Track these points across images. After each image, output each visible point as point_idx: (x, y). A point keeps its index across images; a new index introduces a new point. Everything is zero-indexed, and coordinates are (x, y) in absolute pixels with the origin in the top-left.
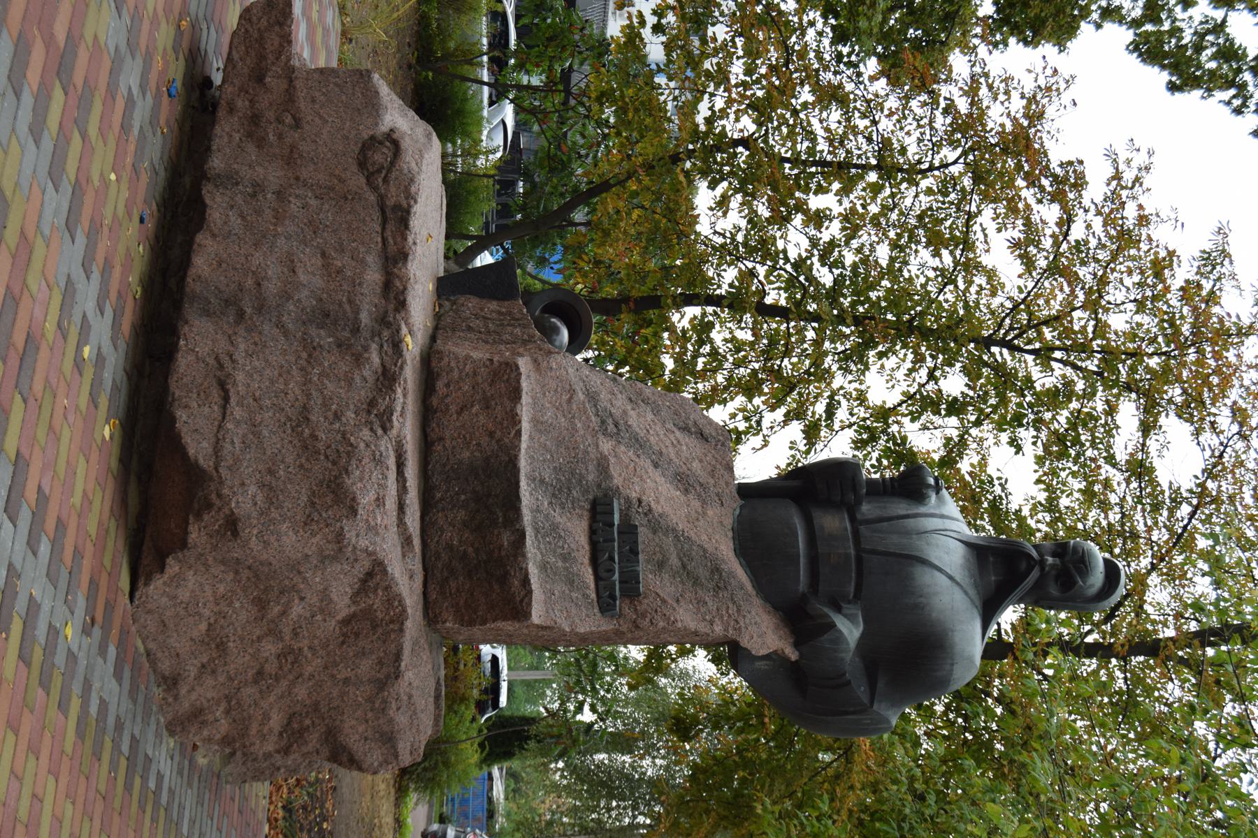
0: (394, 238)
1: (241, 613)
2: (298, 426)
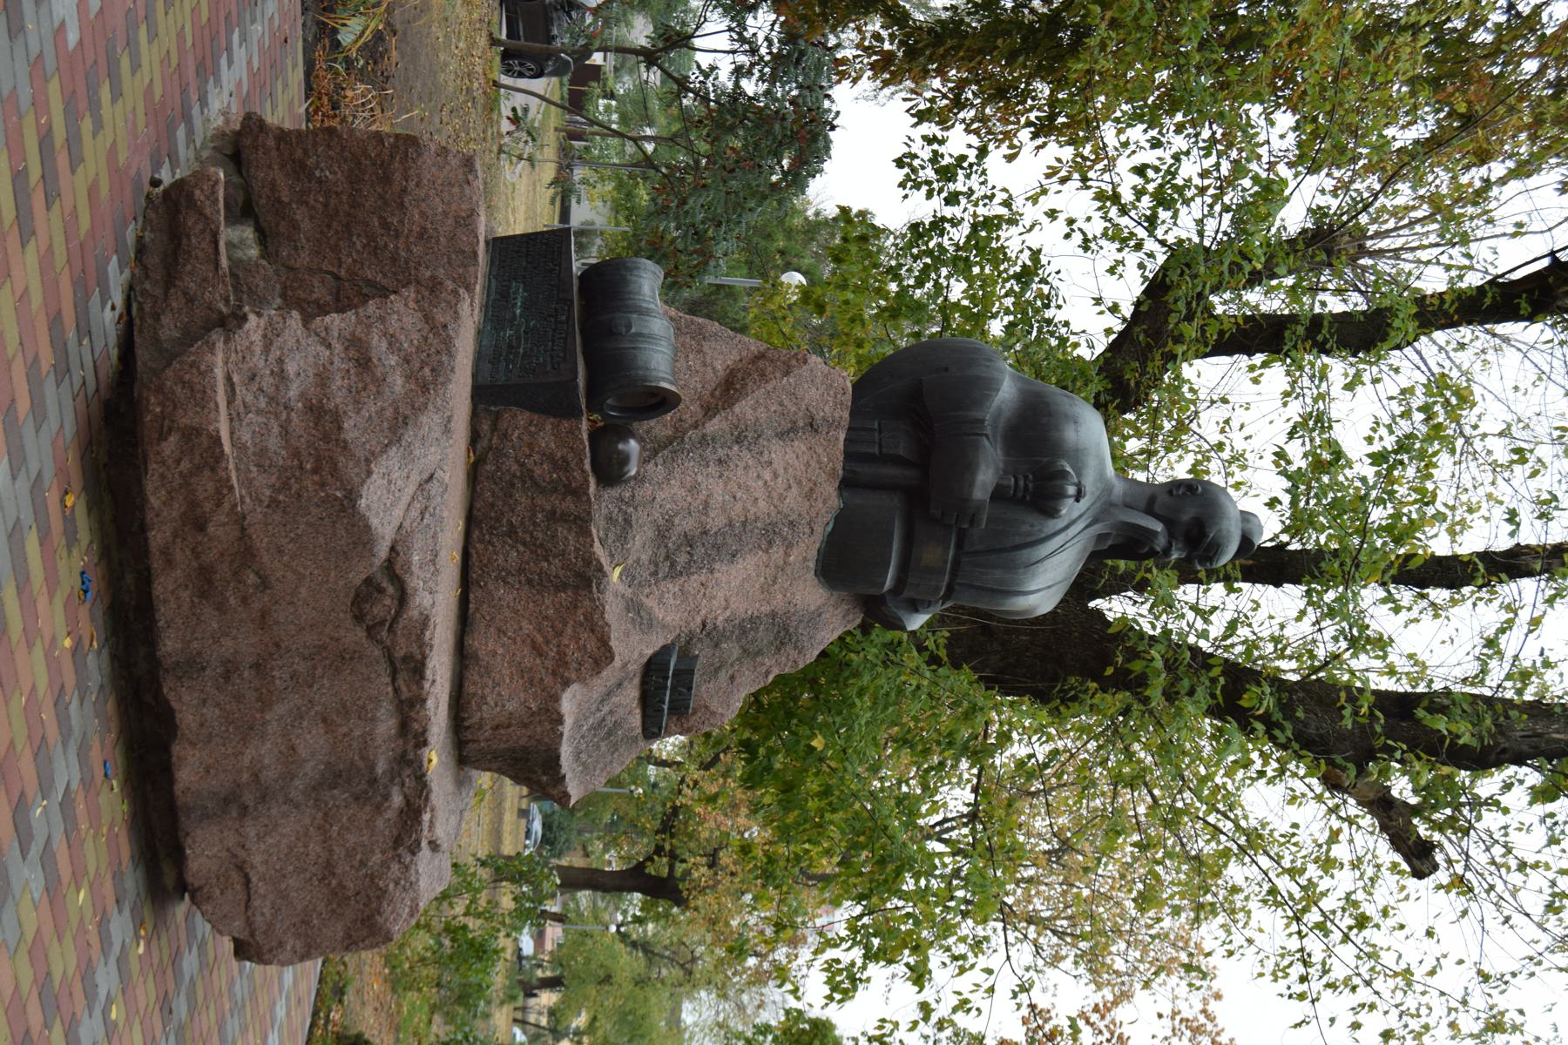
0: (408, 686)
2: (324, 878)
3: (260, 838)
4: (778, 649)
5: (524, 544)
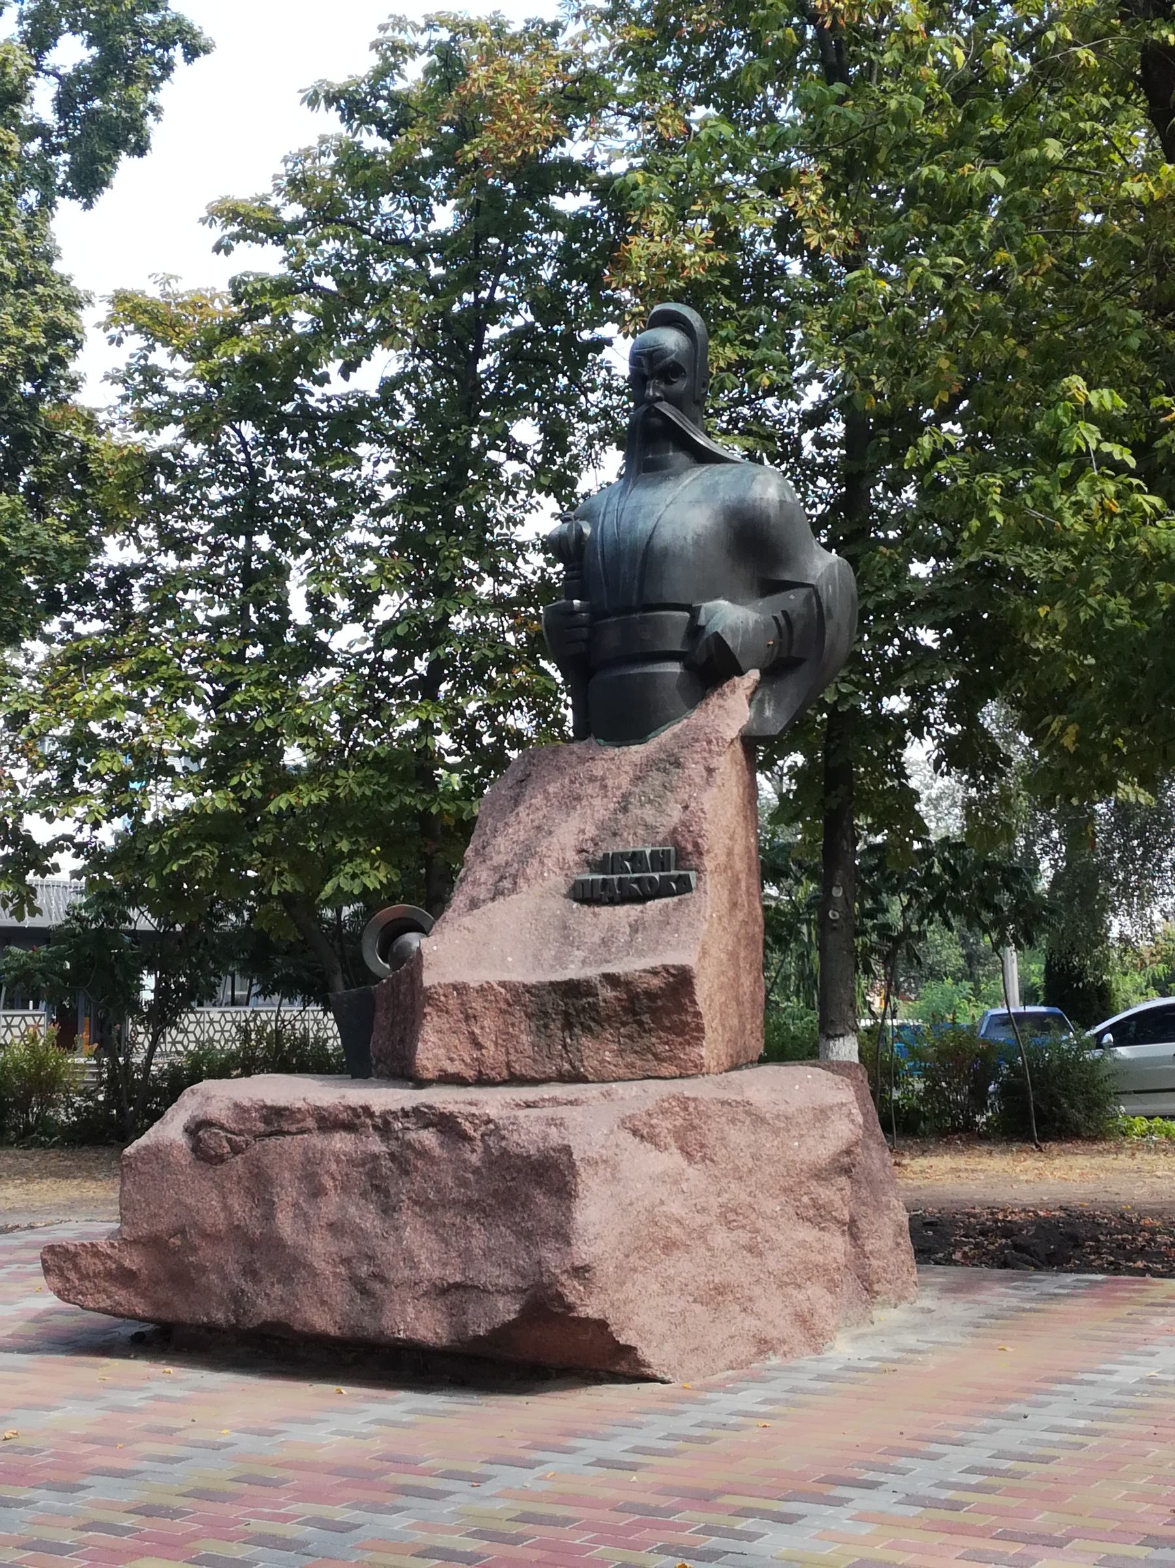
1: (681, 1267)
3: (415, 1266)
4: (678, 764)
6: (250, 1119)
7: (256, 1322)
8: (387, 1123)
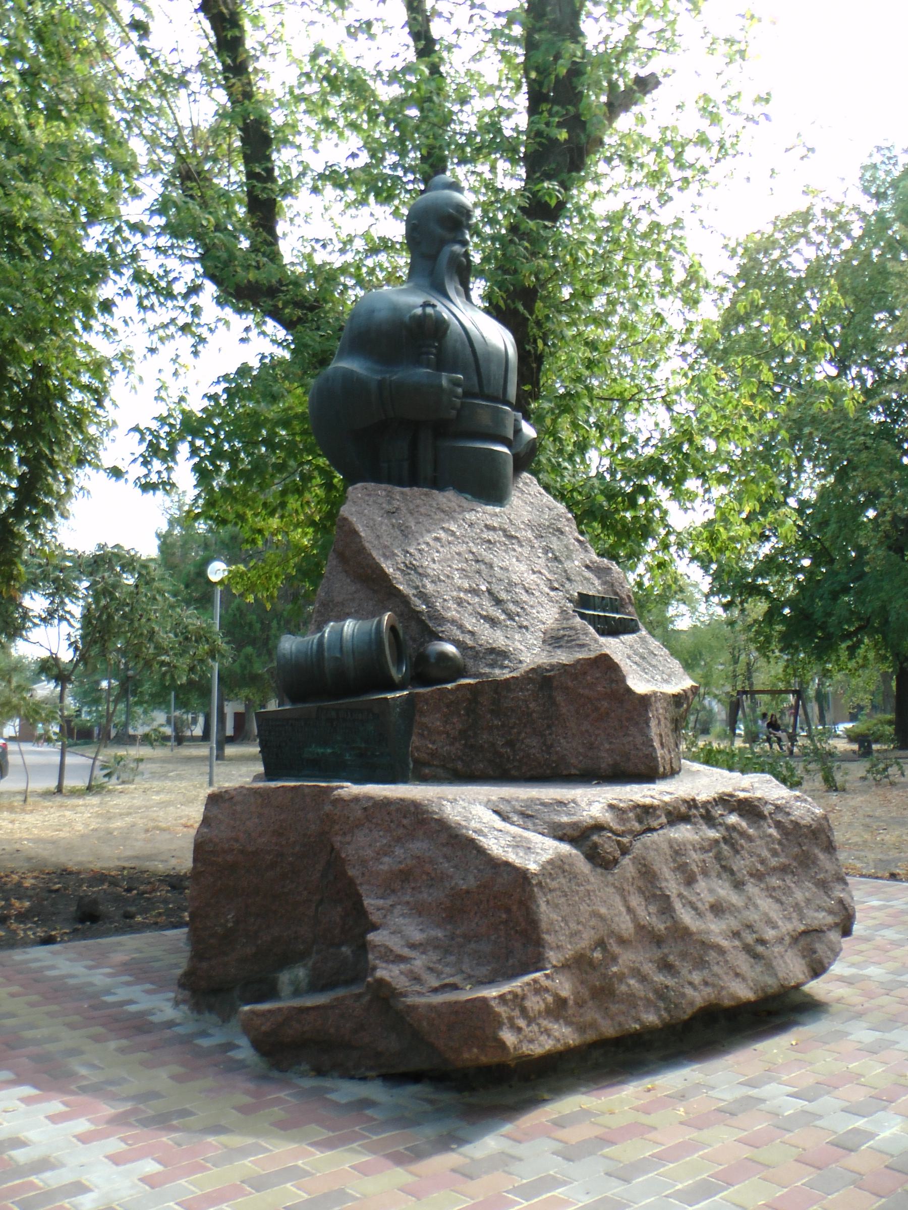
4: (562, 533)
5: (519, 733)
6: (628, 820)
7: (690, 1012)
8: (708, 811)
